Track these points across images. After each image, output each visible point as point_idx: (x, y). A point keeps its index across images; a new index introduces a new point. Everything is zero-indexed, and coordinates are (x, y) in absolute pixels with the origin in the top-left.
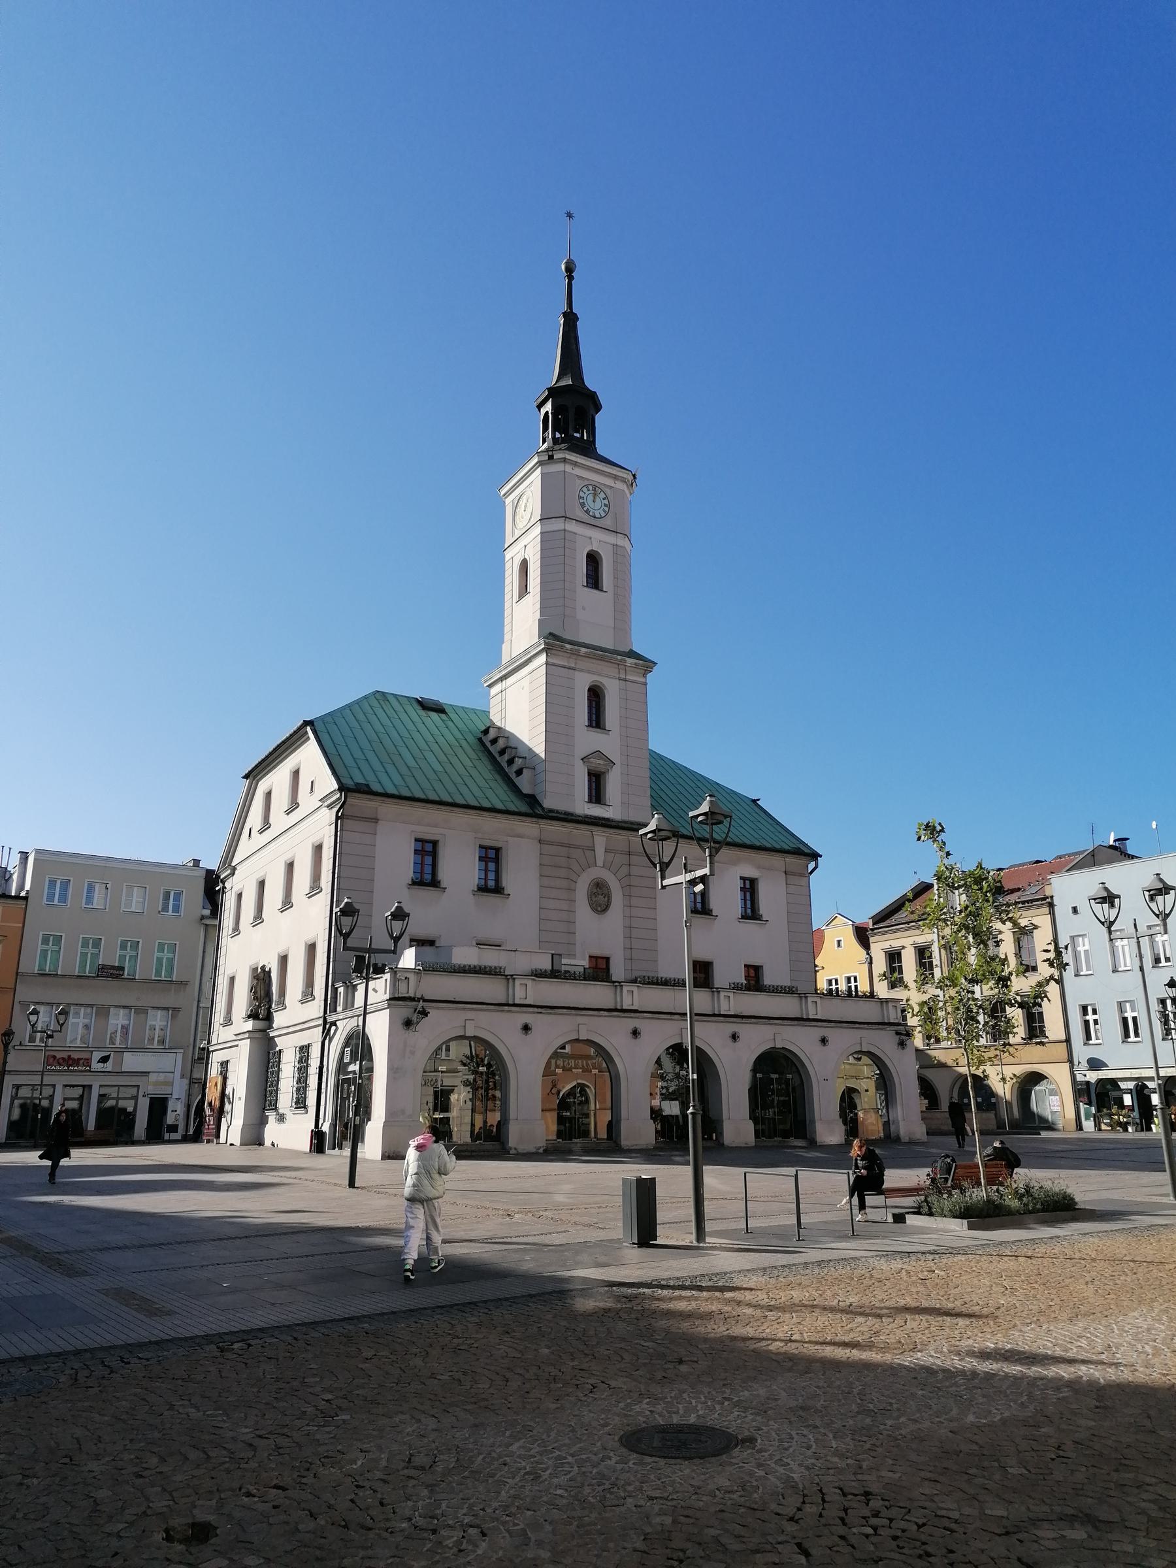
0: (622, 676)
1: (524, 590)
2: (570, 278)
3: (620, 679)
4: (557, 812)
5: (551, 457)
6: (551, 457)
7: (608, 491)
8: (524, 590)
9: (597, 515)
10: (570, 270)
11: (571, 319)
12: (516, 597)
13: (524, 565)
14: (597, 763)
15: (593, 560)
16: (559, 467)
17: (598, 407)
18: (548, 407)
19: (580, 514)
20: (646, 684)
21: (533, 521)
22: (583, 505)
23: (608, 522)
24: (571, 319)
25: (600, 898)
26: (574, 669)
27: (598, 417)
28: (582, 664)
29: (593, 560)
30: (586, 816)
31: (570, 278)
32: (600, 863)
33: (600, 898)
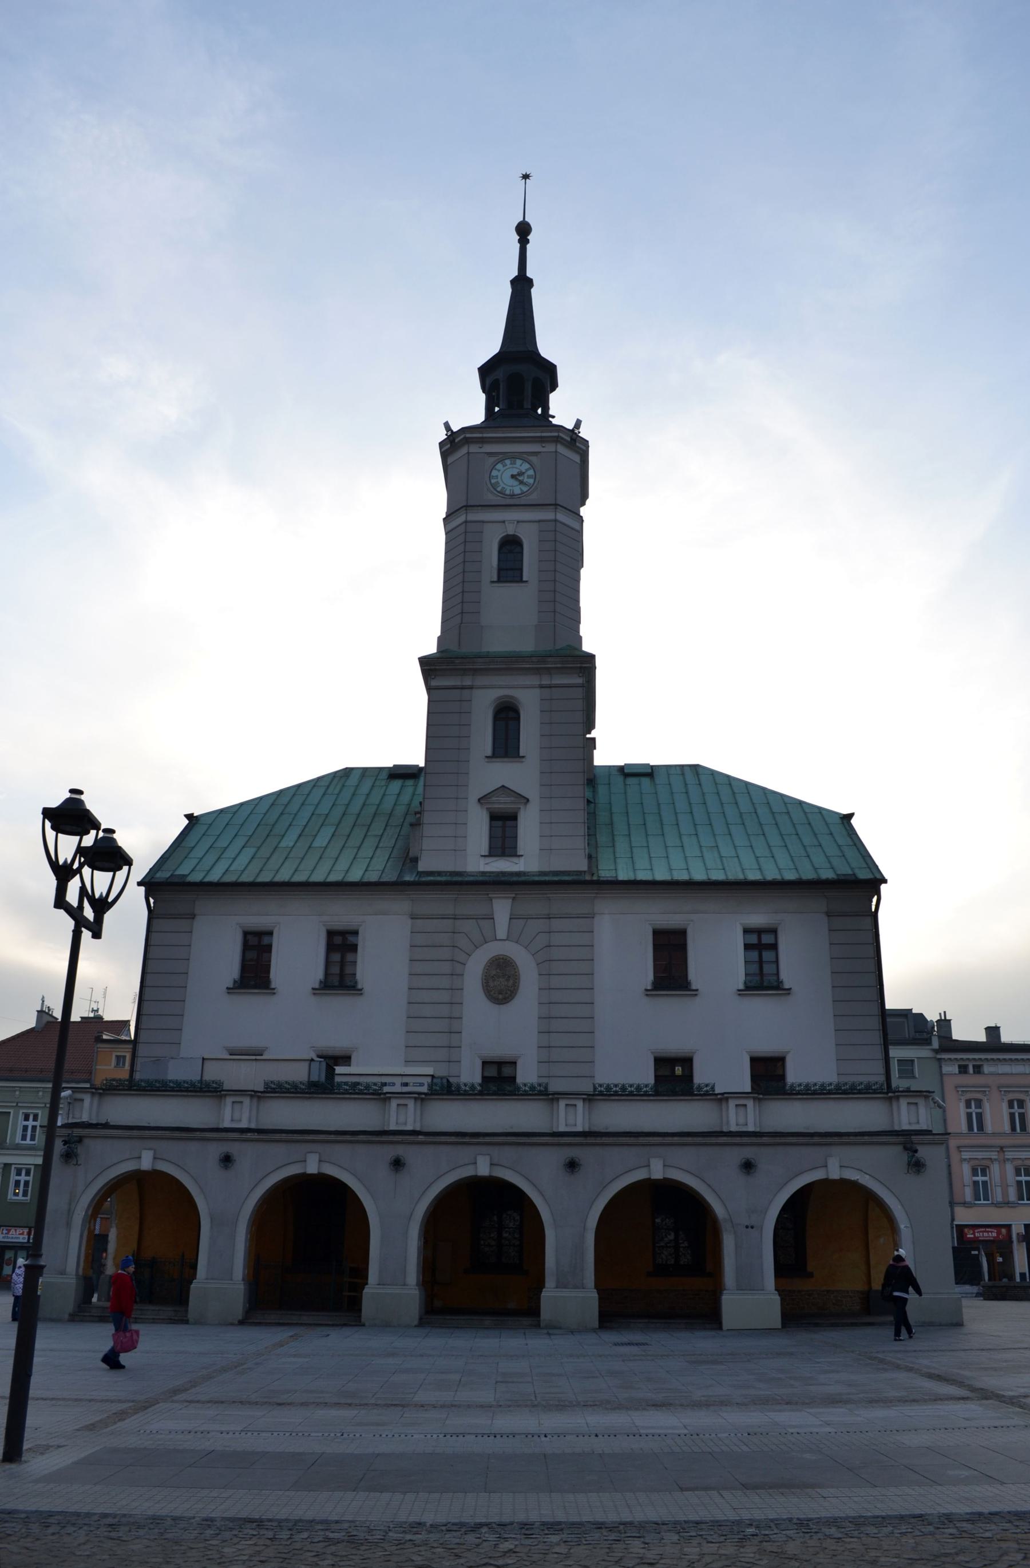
0: (544, 682)
2: (524, 241)
3: (541, 687)
4: (439, 873)
10: (523, 230)
11: (522, 285)
14: (503, 804)
15: (511, 546)
16: (464, 450)
22: (494, 486)
24: (522, 285)
25: (502, 981)
26: (471, 688)
28: (481, 680)
30: (483, 873)
31: (524, 241)
32: (501, 933)
33: (502, 981)
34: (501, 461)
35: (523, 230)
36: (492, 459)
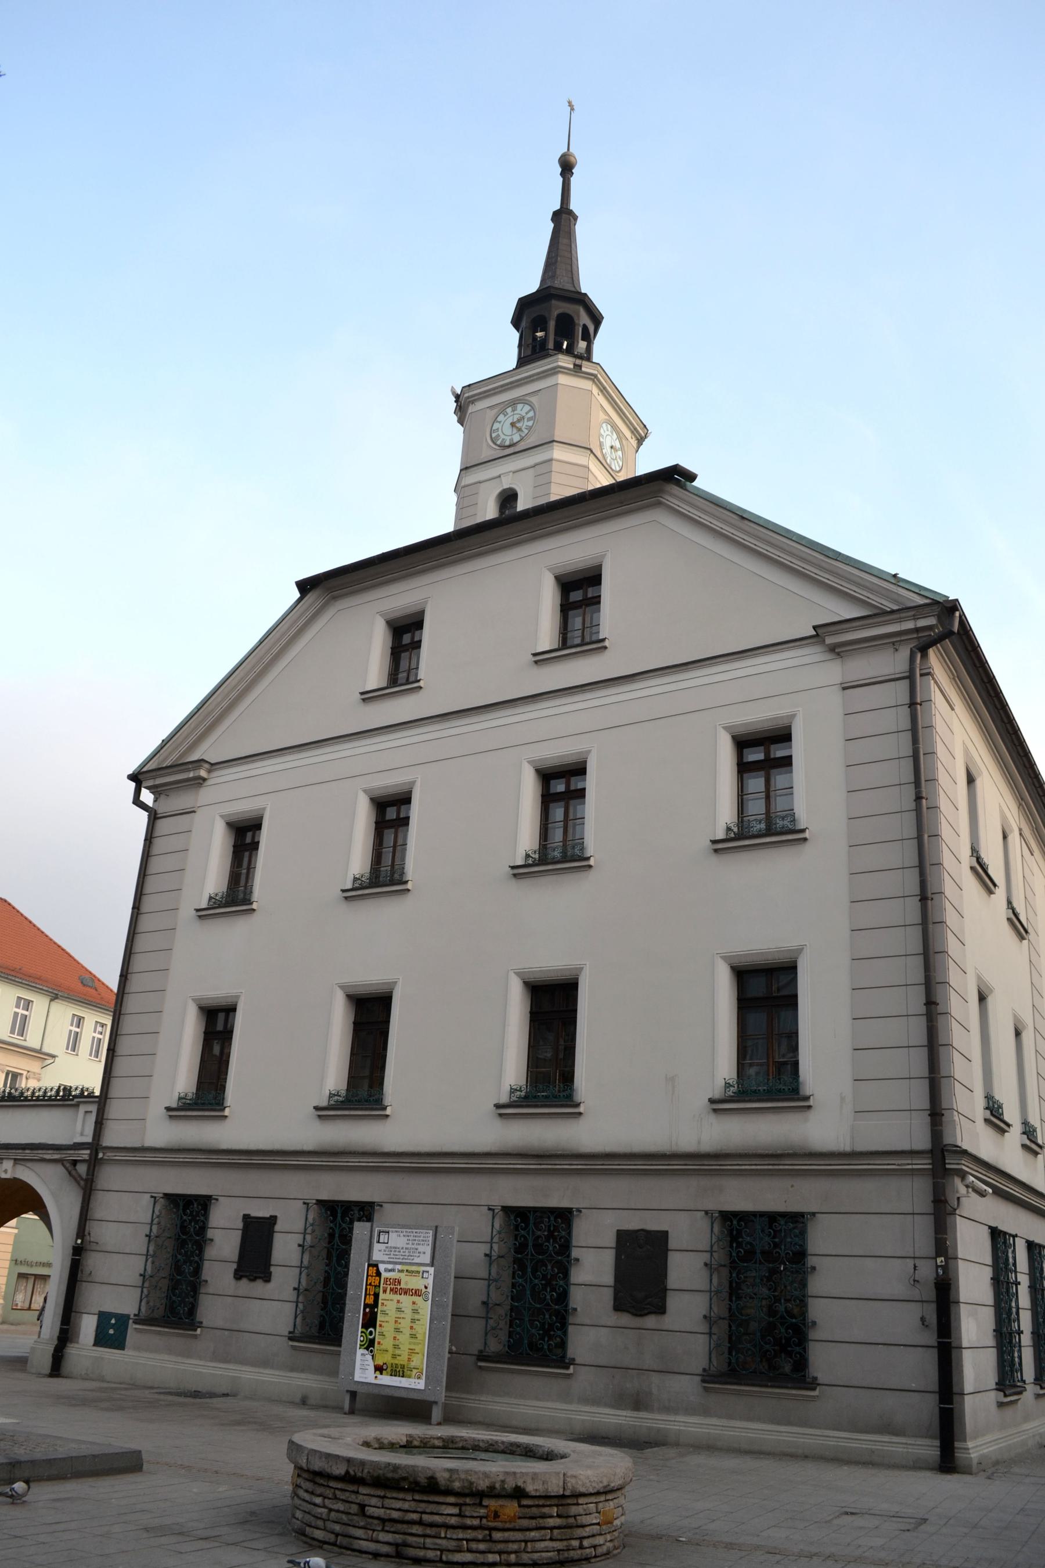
5: (578, 367)
6: (578, 367)
10: (567, 167)
11: (563, 219)
16: (587, 384)
24: (563, 219)
35: (567, 167)
36: (602, 416)
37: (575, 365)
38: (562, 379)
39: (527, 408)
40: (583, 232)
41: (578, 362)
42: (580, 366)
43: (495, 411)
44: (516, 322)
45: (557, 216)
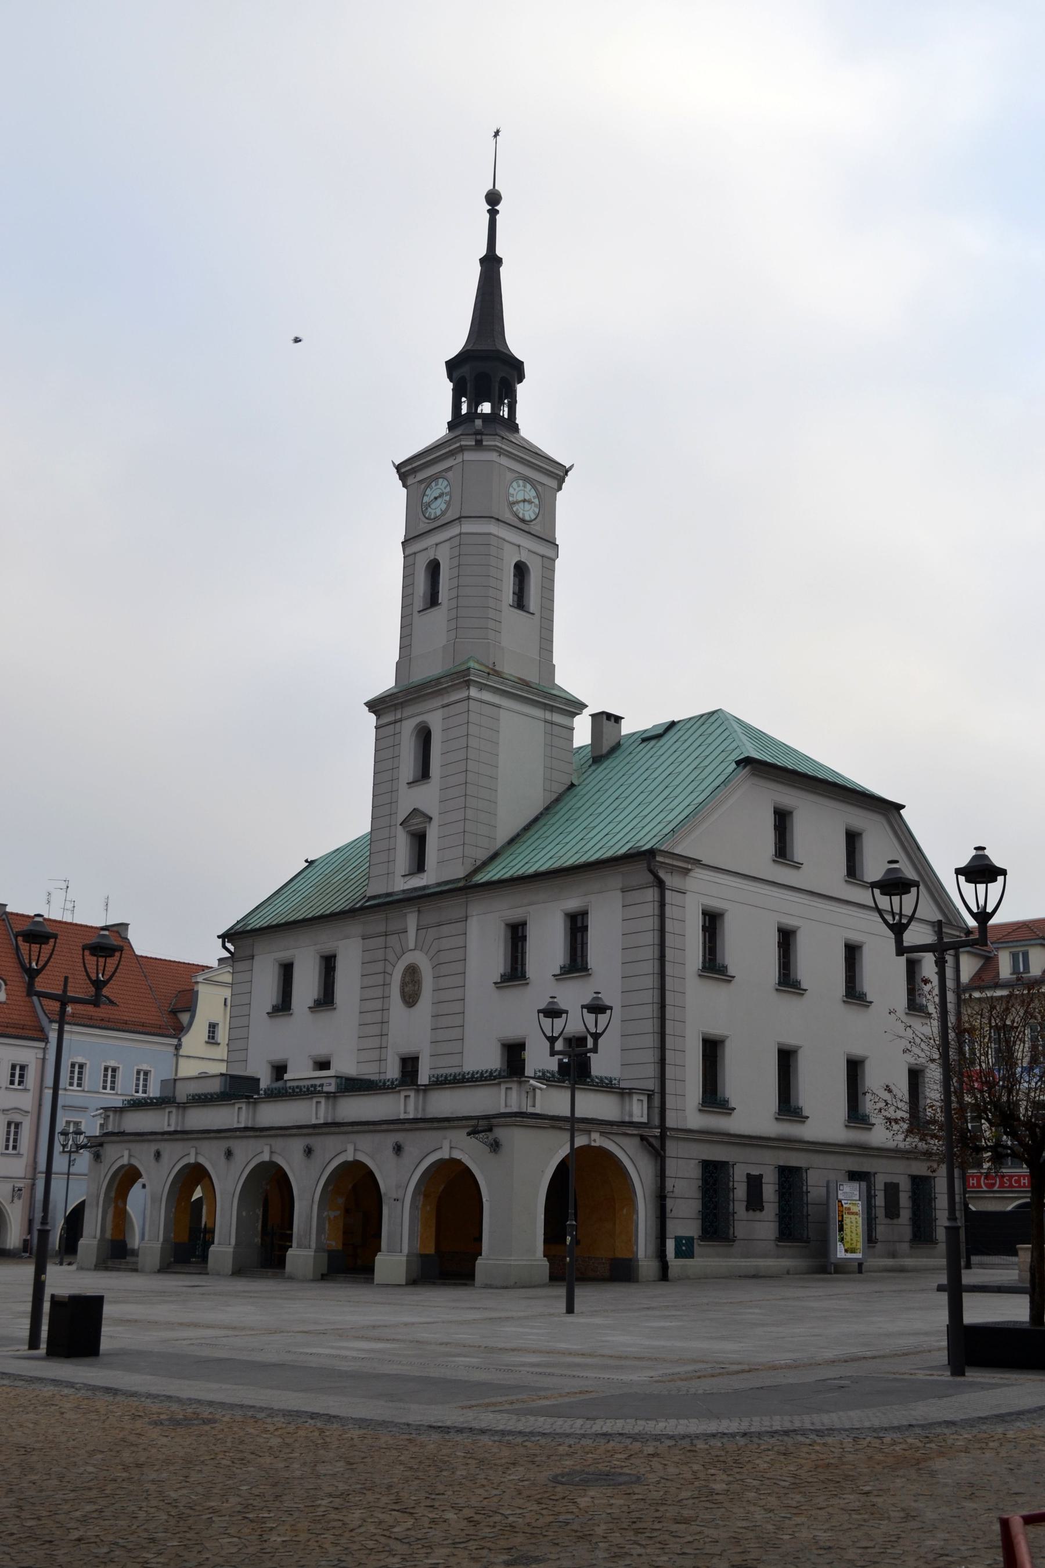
1: (433, 600)
2: (493, 213)
5: (479, 443)
6: (479, 443)
7: (539, 488)
8: (433, 600)
9: (527, 518)
10: (493, 199)
11: (491, 263)
12: (419, 603)
13: (434, 568)
15: (521, 570)
17: (521, 378)
18: (465, 370)
19: (508, 516)
20: (573, 729)
21: (450, 516)
23: (536, 528)
24: (491, 263)
27: (521, 388)
29: (521, 570)
31: (493, 213)
34: (516, 479)
35: (493, 199)
36: (510, 476)
37: (477, 441)
38: (468, 456)
39: (446, 483)
40: (506, 274)
41: (479, 437)
42: (481, 441)
43: (423, 486)
44: (450, 377)
45: (482, 261)
